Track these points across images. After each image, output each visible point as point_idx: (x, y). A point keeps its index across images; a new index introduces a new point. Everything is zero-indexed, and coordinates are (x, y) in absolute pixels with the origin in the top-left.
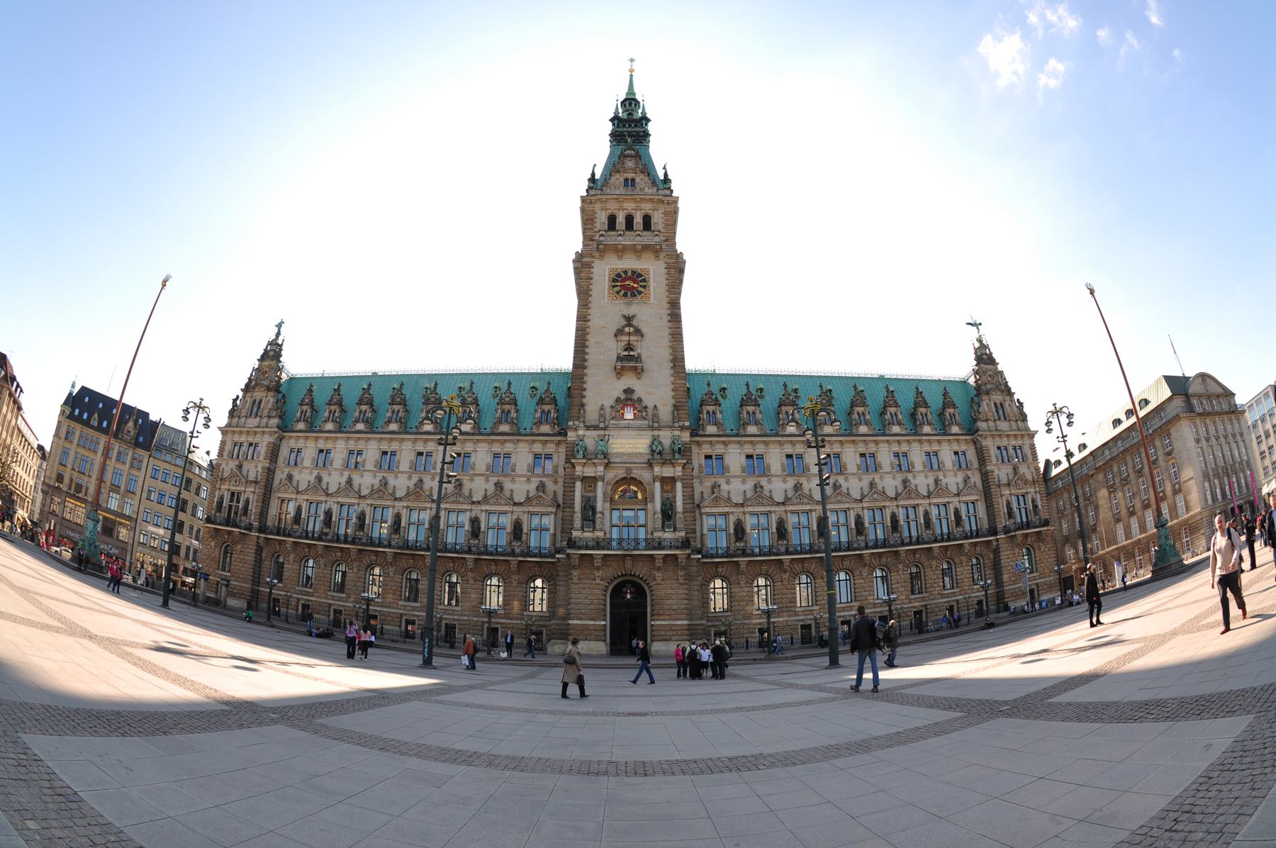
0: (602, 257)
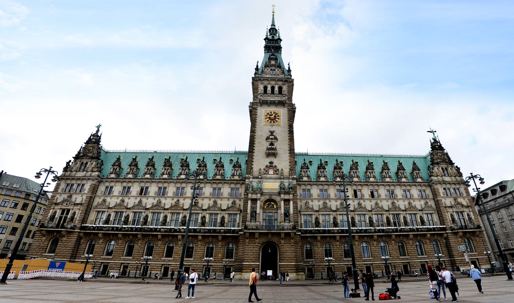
0: (261, 105)
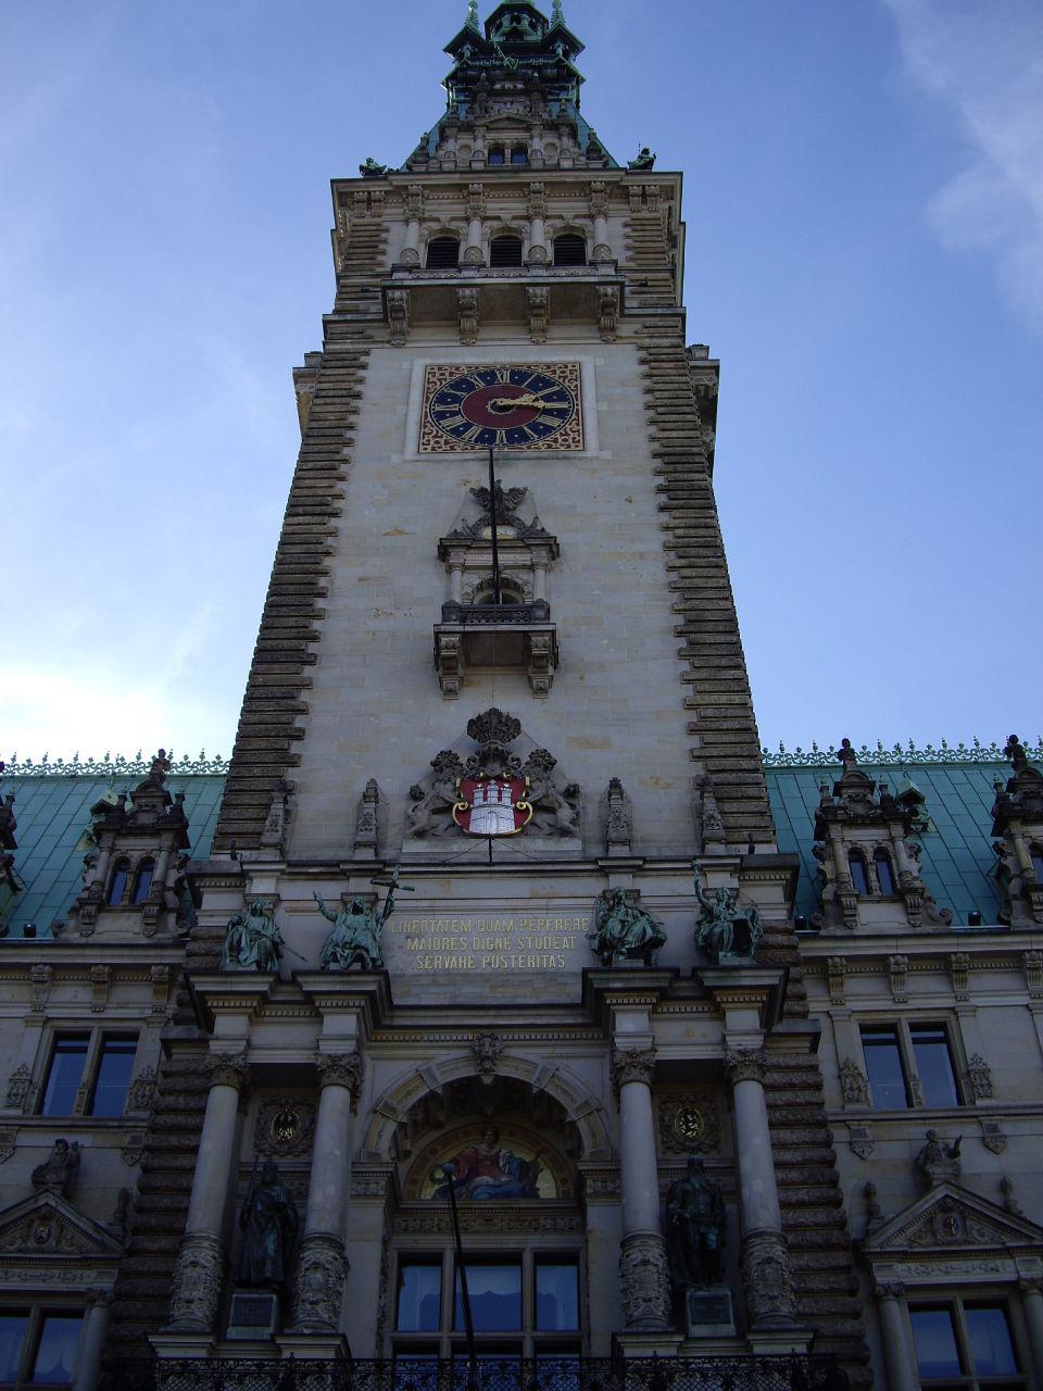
0: (398, 339)
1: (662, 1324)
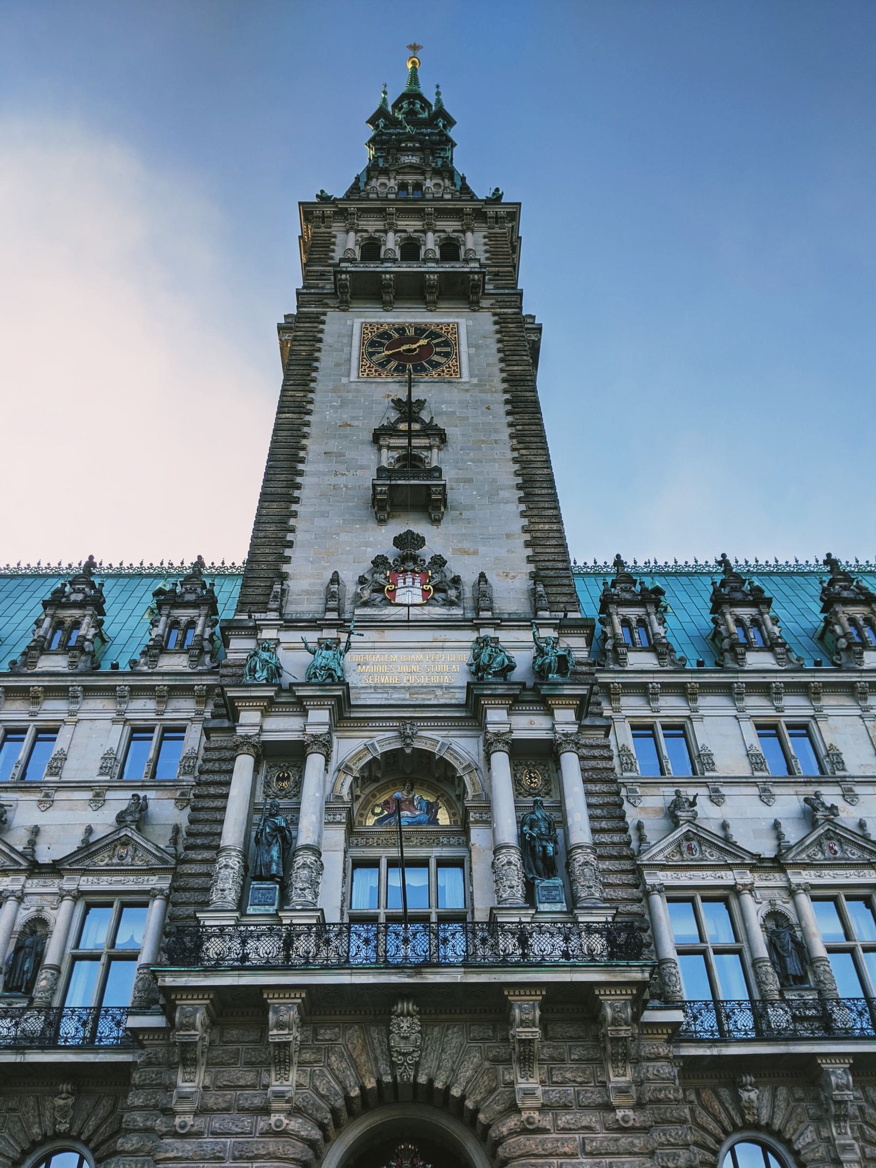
0: (344, 306)
1: (521, 902)
